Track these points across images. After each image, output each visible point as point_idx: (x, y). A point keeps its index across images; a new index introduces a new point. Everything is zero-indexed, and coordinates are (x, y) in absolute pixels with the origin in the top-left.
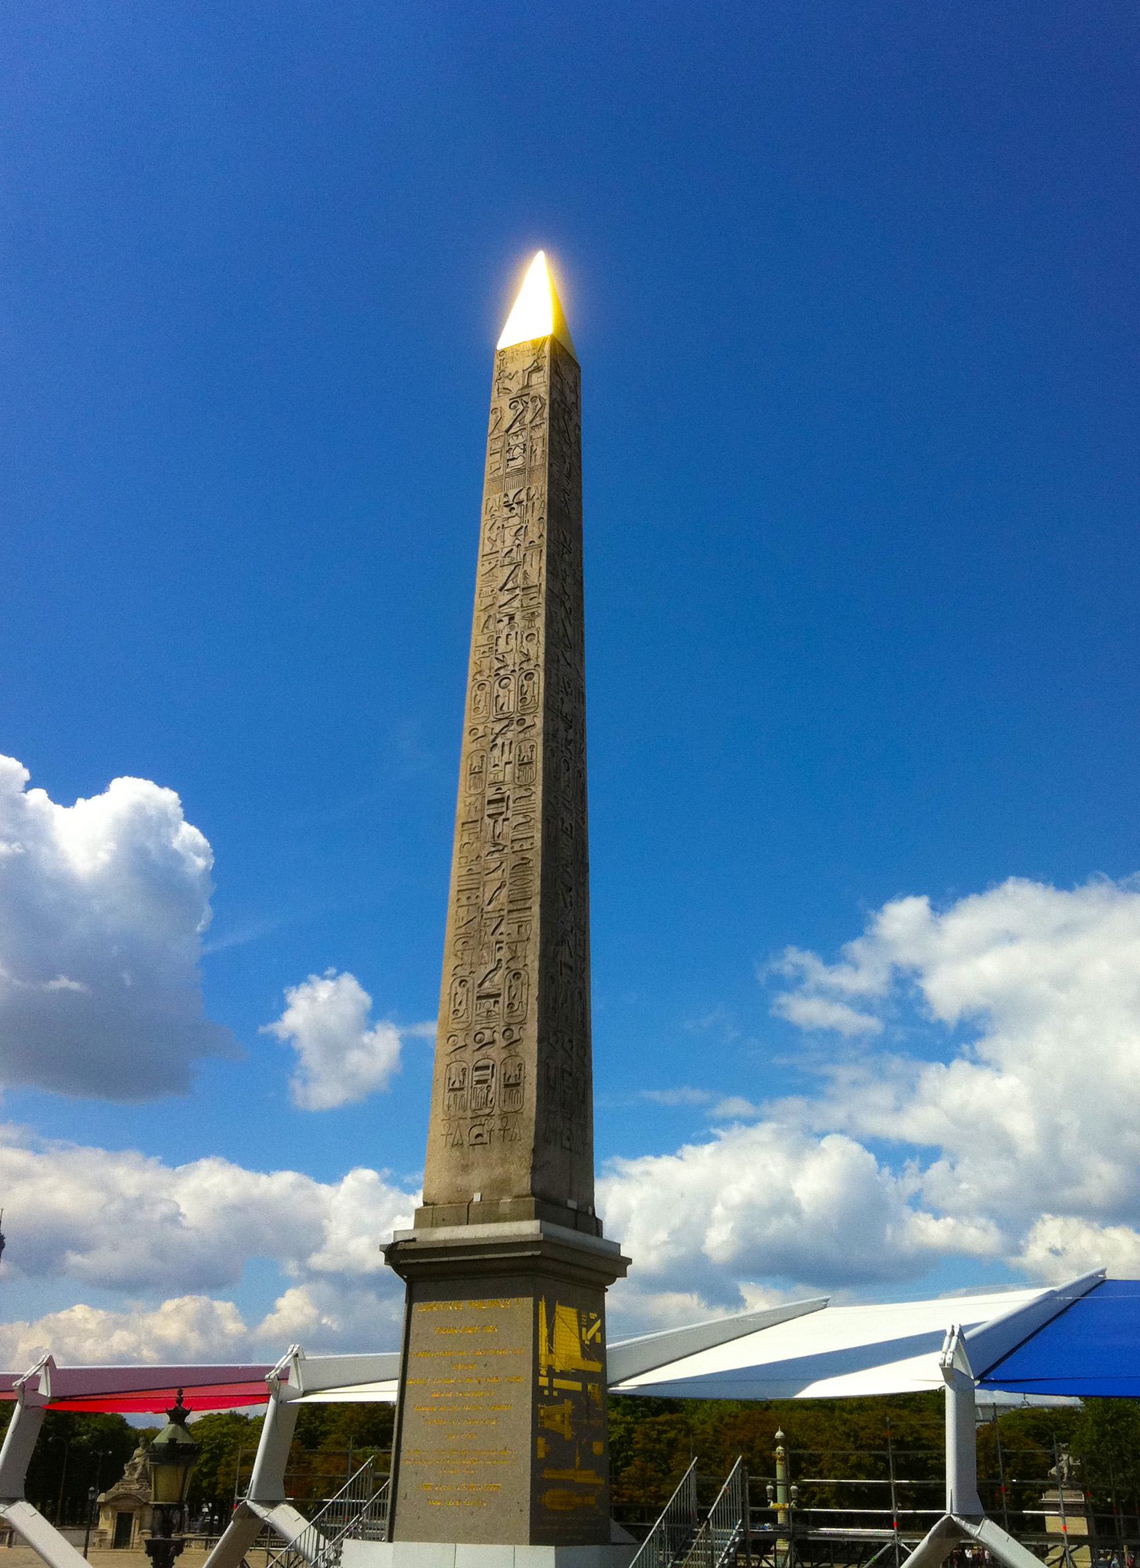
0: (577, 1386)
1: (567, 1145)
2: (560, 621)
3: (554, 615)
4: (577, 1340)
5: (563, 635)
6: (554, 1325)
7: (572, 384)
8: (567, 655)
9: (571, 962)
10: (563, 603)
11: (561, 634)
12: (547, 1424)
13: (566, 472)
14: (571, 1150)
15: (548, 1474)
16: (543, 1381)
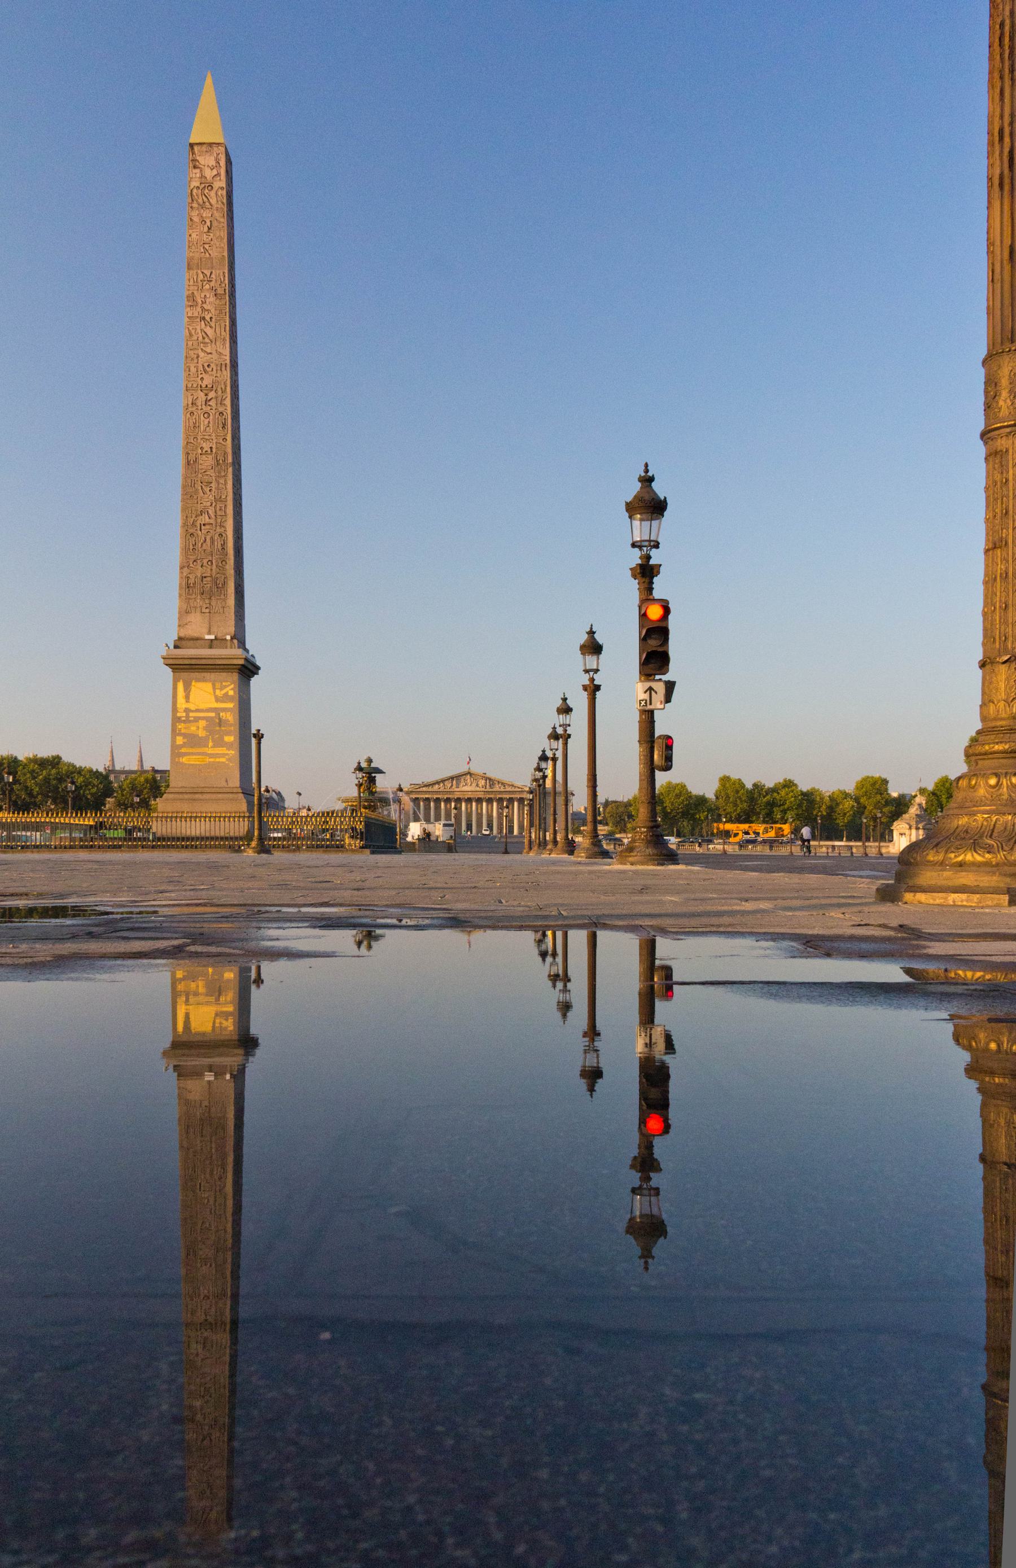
0: (213, 714)
1: (207, 610)
2: (200, 331)
3: (193, 332)
4: (213, 697)
5: (204, 338)
6: (190, 691)
7: (213, 163)
8: (208, 350)
9: (212, 521)
10: (204, 319)
11: (201, 338)
12: (183, 731)
13: (206, 229)
14: (210, 612)
15: (183, 750)
16: (181, 714)
